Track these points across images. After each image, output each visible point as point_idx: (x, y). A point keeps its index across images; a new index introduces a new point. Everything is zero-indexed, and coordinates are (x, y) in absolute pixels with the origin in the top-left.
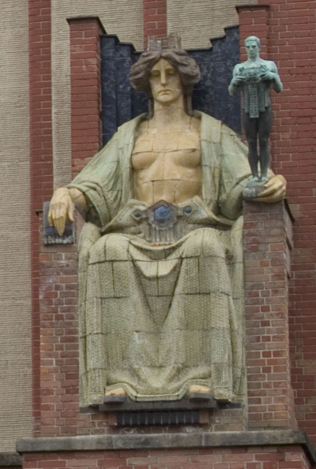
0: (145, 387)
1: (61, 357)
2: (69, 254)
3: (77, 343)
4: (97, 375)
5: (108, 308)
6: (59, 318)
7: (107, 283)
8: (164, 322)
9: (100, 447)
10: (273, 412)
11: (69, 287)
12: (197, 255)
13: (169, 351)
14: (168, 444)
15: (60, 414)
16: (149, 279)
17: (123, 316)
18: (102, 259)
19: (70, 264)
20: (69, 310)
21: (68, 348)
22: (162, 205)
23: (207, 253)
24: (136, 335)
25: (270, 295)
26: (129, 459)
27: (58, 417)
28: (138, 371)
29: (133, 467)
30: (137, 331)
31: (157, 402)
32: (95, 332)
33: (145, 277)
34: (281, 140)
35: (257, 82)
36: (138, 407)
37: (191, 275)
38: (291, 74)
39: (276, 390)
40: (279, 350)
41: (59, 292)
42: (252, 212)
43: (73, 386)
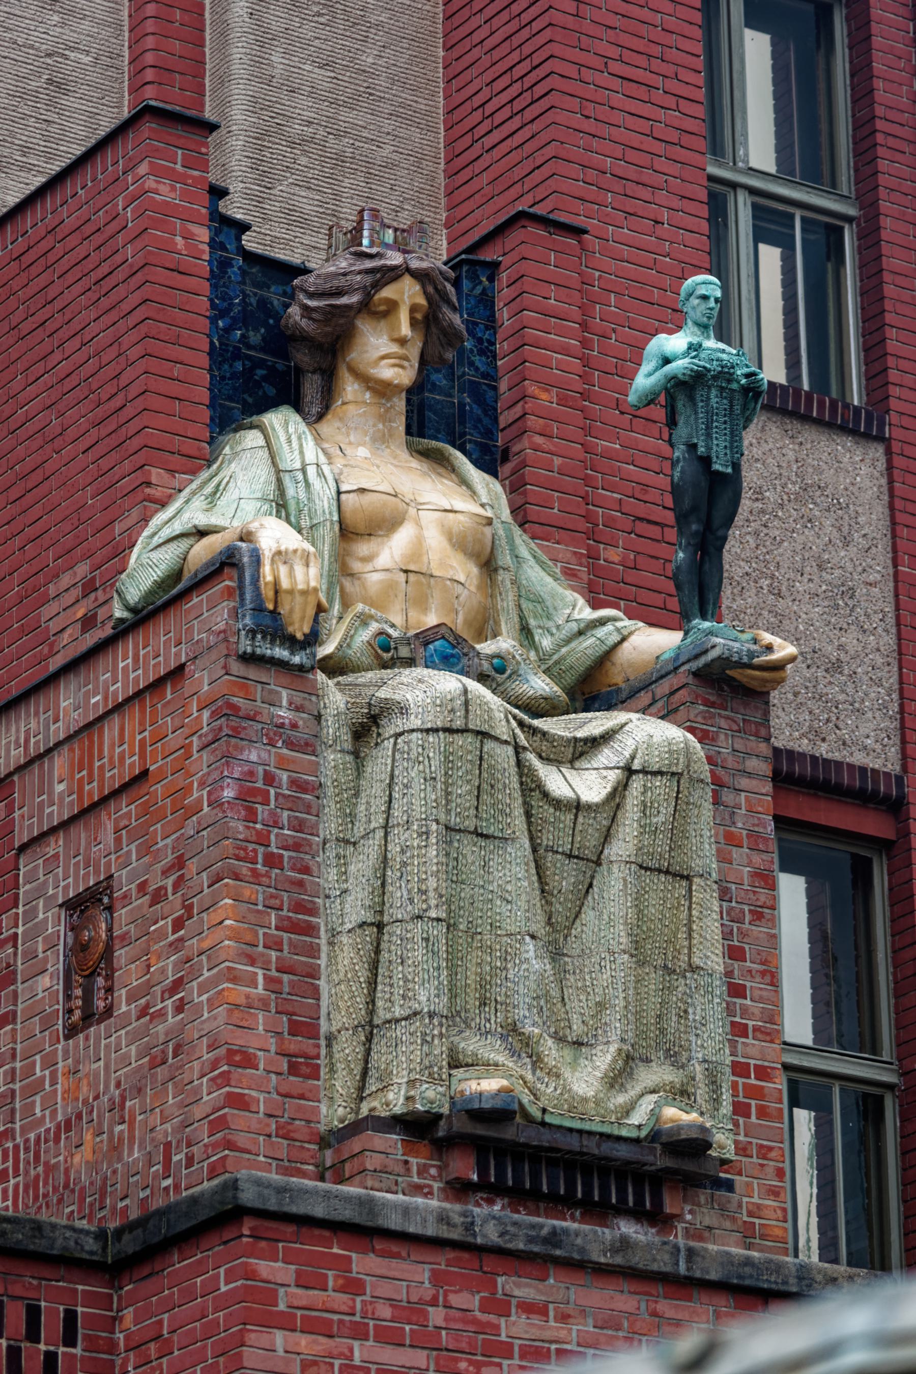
0: (556, 1089)
1: (278, 970)
2: (298, 698)
3: (317, 941)
4: (436, 1032)
5: (457, 859)
6: (272, 861)
7: (463, 791)
8: (569, 928)
9: (445, 1233)
10: (757, 1221)
11: (295, 784)
12: (674, 769)
13: (601, 1006)
14: (605, 1255)
15: (274, 1126)
16: (558, 804)
17: (491, 888)
18: (458, 723)
19: (301, 723)
20: (296, 847)
21: (295, 949)
22: (443, 638)
23: (695, 772)
24: (530, 945)
25: (747, 921)
26: (504, 1278)
27: (269, 1136)
28: (538, 1042)
29: (514, 1302)
30: (533, 937)
31: (590, 1133)
32: (433, 914)
33: (546, 795)
34: (602, 562)
35: (735, 386)
36: (545, 1139)
37: (655, 820)
38: (622, 413)
39: (762, 1165)
40: (766, 1064)
41: (272, 792)
42: (707, 703)
43: (306, 1057)
